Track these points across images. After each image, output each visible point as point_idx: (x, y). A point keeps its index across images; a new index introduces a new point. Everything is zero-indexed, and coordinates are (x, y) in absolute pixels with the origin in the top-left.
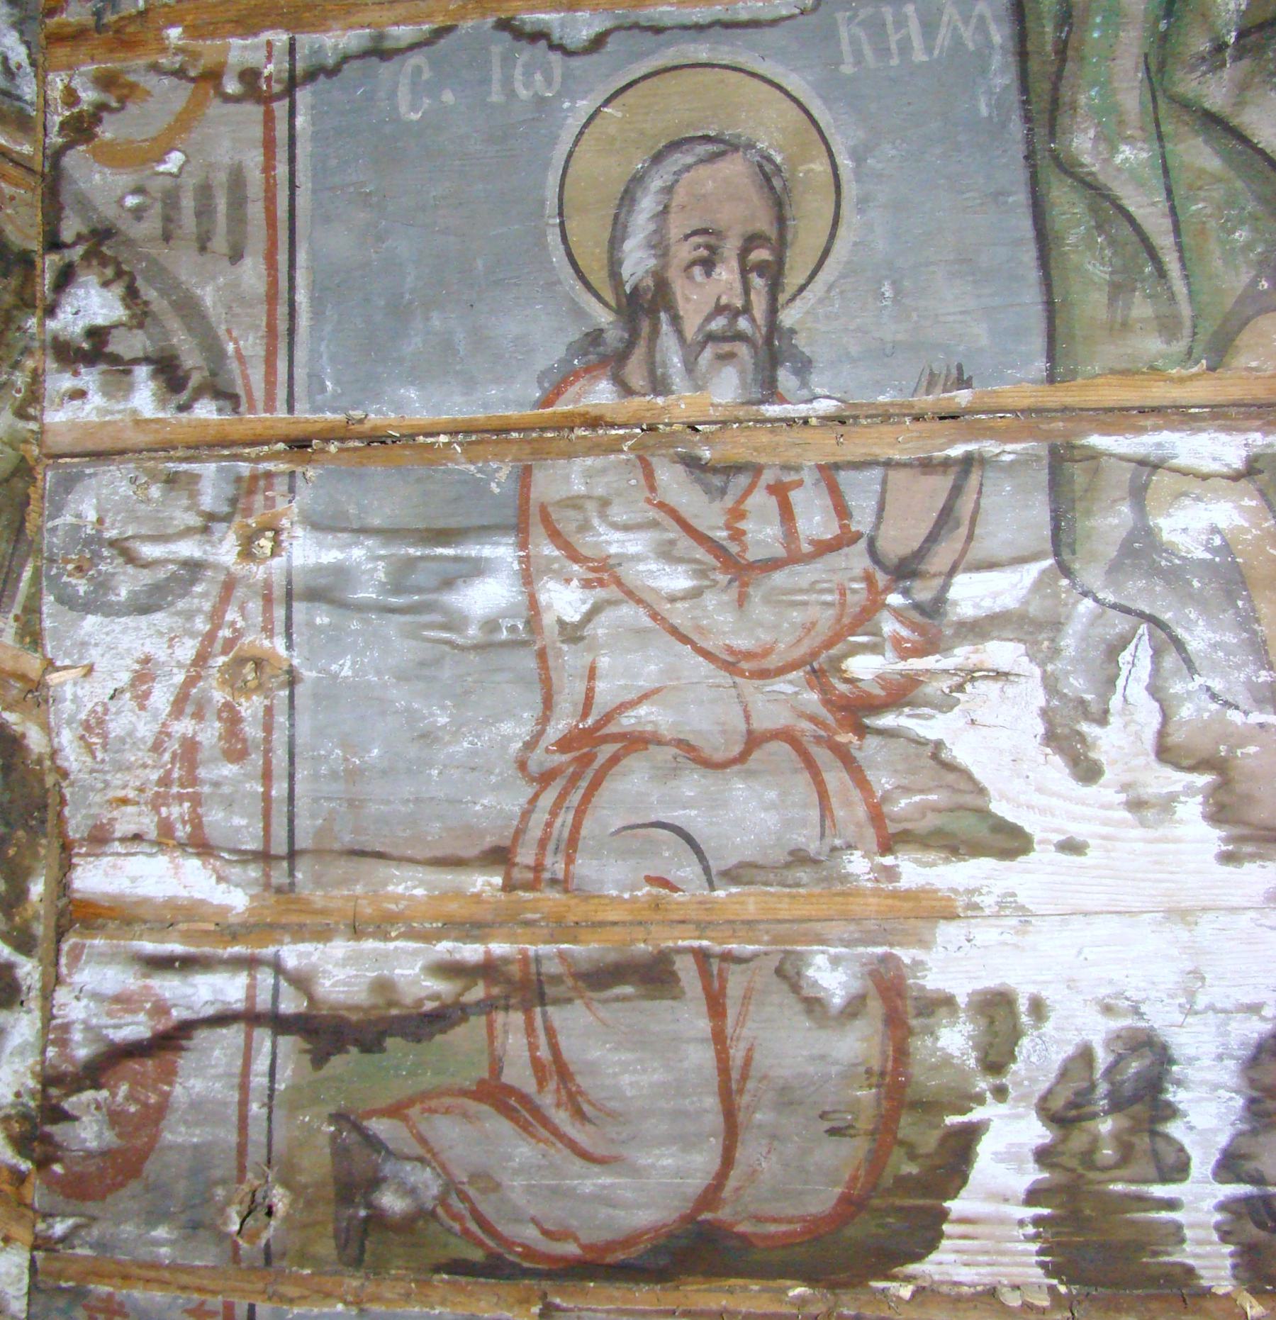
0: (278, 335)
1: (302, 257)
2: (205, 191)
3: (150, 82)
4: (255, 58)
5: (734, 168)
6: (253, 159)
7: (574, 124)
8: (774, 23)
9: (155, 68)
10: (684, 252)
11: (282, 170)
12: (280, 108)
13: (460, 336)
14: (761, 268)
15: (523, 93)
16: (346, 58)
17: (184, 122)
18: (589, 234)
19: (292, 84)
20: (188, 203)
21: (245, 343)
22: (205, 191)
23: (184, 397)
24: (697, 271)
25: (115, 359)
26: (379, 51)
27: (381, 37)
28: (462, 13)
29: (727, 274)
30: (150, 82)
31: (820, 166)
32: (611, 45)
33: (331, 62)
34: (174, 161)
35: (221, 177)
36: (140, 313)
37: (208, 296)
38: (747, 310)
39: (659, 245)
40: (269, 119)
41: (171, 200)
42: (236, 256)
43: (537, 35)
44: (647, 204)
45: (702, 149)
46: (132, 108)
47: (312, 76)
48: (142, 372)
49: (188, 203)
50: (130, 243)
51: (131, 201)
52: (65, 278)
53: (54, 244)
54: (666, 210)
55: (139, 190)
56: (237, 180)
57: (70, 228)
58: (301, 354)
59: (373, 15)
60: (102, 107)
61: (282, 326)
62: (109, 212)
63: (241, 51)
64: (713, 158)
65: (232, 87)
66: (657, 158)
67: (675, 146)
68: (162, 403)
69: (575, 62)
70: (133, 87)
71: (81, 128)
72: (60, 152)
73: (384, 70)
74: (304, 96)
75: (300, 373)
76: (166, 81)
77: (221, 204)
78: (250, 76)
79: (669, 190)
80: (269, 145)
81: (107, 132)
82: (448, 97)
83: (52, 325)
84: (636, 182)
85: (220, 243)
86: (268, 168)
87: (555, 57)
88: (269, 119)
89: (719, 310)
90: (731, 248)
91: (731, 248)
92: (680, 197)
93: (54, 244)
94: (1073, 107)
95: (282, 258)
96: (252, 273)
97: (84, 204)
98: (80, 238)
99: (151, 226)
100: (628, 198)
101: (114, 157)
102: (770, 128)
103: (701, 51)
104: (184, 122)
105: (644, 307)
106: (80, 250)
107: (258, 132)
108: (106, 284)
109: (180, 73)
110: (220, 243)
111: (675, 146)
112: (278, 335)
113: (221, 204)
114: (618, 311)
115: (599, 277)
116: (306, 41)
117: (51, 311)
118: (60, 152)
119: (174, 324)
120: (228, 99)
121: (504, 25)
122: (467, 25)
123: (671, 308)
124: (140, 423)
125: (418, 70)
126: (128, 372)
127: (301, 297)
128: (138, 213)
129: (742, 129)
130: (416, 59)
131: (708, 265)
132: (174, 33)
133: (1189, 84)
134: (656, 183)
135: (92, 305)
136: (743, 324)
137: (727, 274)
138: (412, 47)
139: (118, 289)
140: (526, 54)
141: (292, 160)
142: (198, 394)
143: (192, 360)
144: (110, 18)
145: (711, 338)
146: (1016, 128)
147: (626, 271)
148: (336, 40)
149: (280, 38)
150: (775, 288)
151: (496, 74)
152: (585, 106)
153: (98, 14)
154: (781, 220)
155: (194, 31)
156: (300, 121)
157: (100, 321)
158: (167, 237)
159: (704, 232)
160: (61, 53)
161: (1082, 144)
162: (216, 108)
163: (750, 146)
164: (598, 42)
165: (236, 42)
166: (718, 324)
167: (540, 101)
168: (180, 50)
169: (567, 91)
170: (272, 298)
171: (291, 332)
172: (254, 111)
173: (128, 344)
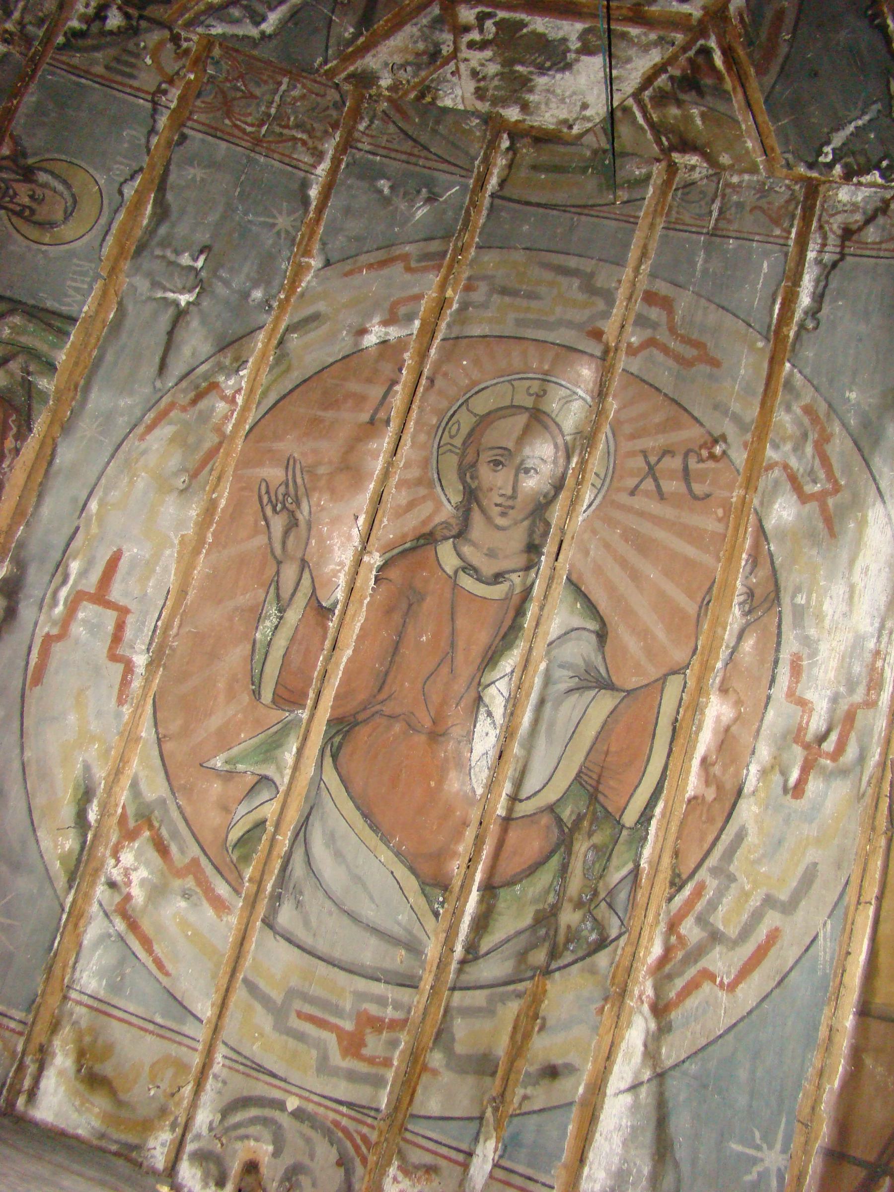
0: (74, 70)
1: (97, 86)
2: (132, 66)
3: (180, 63)
4: (169, 97)
5: (60, 216)
6: (136, 84)
7: (97, 177)
8: (101, 246)
9: (184, 67)
10: (39, 192)
11: (128, 90)
12: (149, 98)
13: (45, 119)
14: (22, 211)
15: (116, 166)
16: (155, 121)
17: (160, 69)
18: (58, 167)
19: (155, 103)
20: (133, 60)
21: (77, 59)
22: (132, 66)
23: (69, 35)
24: (31, 193)
25: (93, 20)
26: (152, 131)
27: (157, 133)
28: (152, 159)
29: (26, 201)
30: (180, 63)
31: (47, 240)
32: (118, 196)
33: (157, 117)
34: (149, 61)
35: (135, 73)
36: (103, 33)
37: (98, 55)
38: (11, 202)
39: (45, 186)
40: (147, 93)
41: (137, 56)
42: (107, 68)
43: (132, 177)
44: (60, 188)
45: (70, 210)
46: (173, 55)
47: (155, 110)
48: (84, 27)
49: (133, 60)
50: (130, 38)
51: (142, 44)
52: (127, 16)
53: (141, 17)
54: (55, 191)
55: (145, 48)
56: (132, 76)
57: (144, 24)
58: (65, 74)
59: (166, 133)
60: (179, 47)
61: (77, 72)
62: (141, 37)
63: (175, 93)
64: (65, 212)
65: (164, 86)
66: (73, 196)
67: (75, 202)
68: (70, 29)
69: (117, 186)
70: (181, 59)
71: (176, 39)
72: (171, 30)
73: (146, 131)
74: (149, 105)
75: (58, 71)
76: (177, 68)
77: (127, 70)
78: (165, 92)
79: (61, 195)
80: (138, 90)
81: (170, 46)
82: (126, 145)
83: (115, 7)
84: (69, 187)
85: (114, 65)
86: (131, 87)
87: (122, 180)
88: (147, 93)
89: (16, 194)
90: (34, 206)
91: (34, 206)
92: (58, 198)
93: (141, 17)
94: (30, 321)
95: (99, 80)
96: (99, 70)
97: (148, 30)
98: (138, 25)
99: (131, 46)
100: (65, 182)
101: (161, 44)
102: (67, 231)
103: (103, 221)
104: (160, 69)
105: (28, 174)
106: (134, 23)
107: (145, 88)
108: (119, 27)
109: (177, 73)
110: (114, 65)
111: (75, 202)
112: (74, 70)
113: (127, 70)
114: (29, 166)
115: (44, 165)
116: (167, 113)
117: (120, 8)
118: (171, 30)
119: (95, 42)
120: (160, 85)
121: (141, 169)
122: (147, 159)
123: (24, 181)
124: (68, 19)
125: (139, 140)
126: (86, 23)
127: (83, 81)
128: (138, 45)
129: (71, 224)
130: (143, 141)
131: (32, 197)
132: (192, 77)
133: (20, 359)
134: (66, 193)
135: (115, 20)
136: (8, 199)
137: (26, 201)
138: (148, 141)
139: (115, 30)
140: (127, 171)
141: (129, 94)
142: (68, 40)
143: (80, 42)
144: (209, 61)
145: (8, 188)
146: (31, 302)
147: (41, 173)
148: (163, 121)
149: (173, 106)
150: (15, 213)
151: (125, 161)
152: (102, 182)
153: (213, 58)
154: (35, 223)
155: (189, 82)
156: (141, 101)
157: (108, 21)
158: (124, 50)
159: (43, 200)
160: (205, 42)
161: (17, 320)
162: (159, 79)
163: (64, 223)
164: (121, 193)
165: (179, 92)
166: (11, 192)
167: (110, 170)
168: (185, 76)
169: (110, 180)
170: (87, 72)
171: (73, 74)
172: (152, 90)
173: (95, 27)
